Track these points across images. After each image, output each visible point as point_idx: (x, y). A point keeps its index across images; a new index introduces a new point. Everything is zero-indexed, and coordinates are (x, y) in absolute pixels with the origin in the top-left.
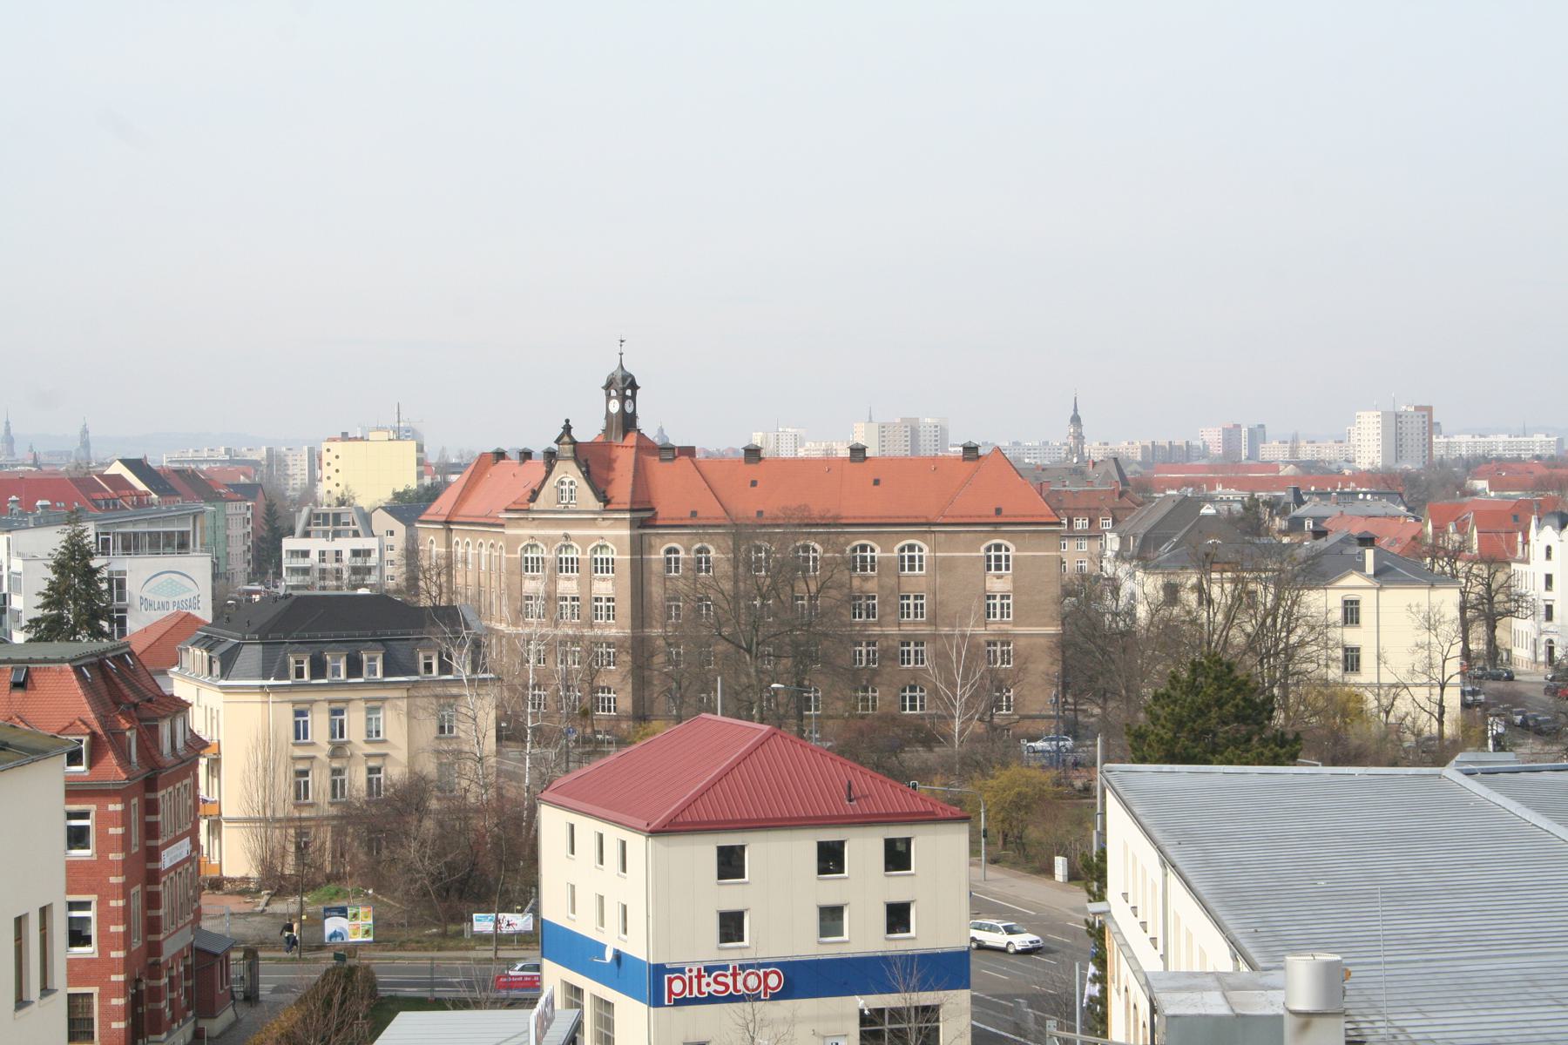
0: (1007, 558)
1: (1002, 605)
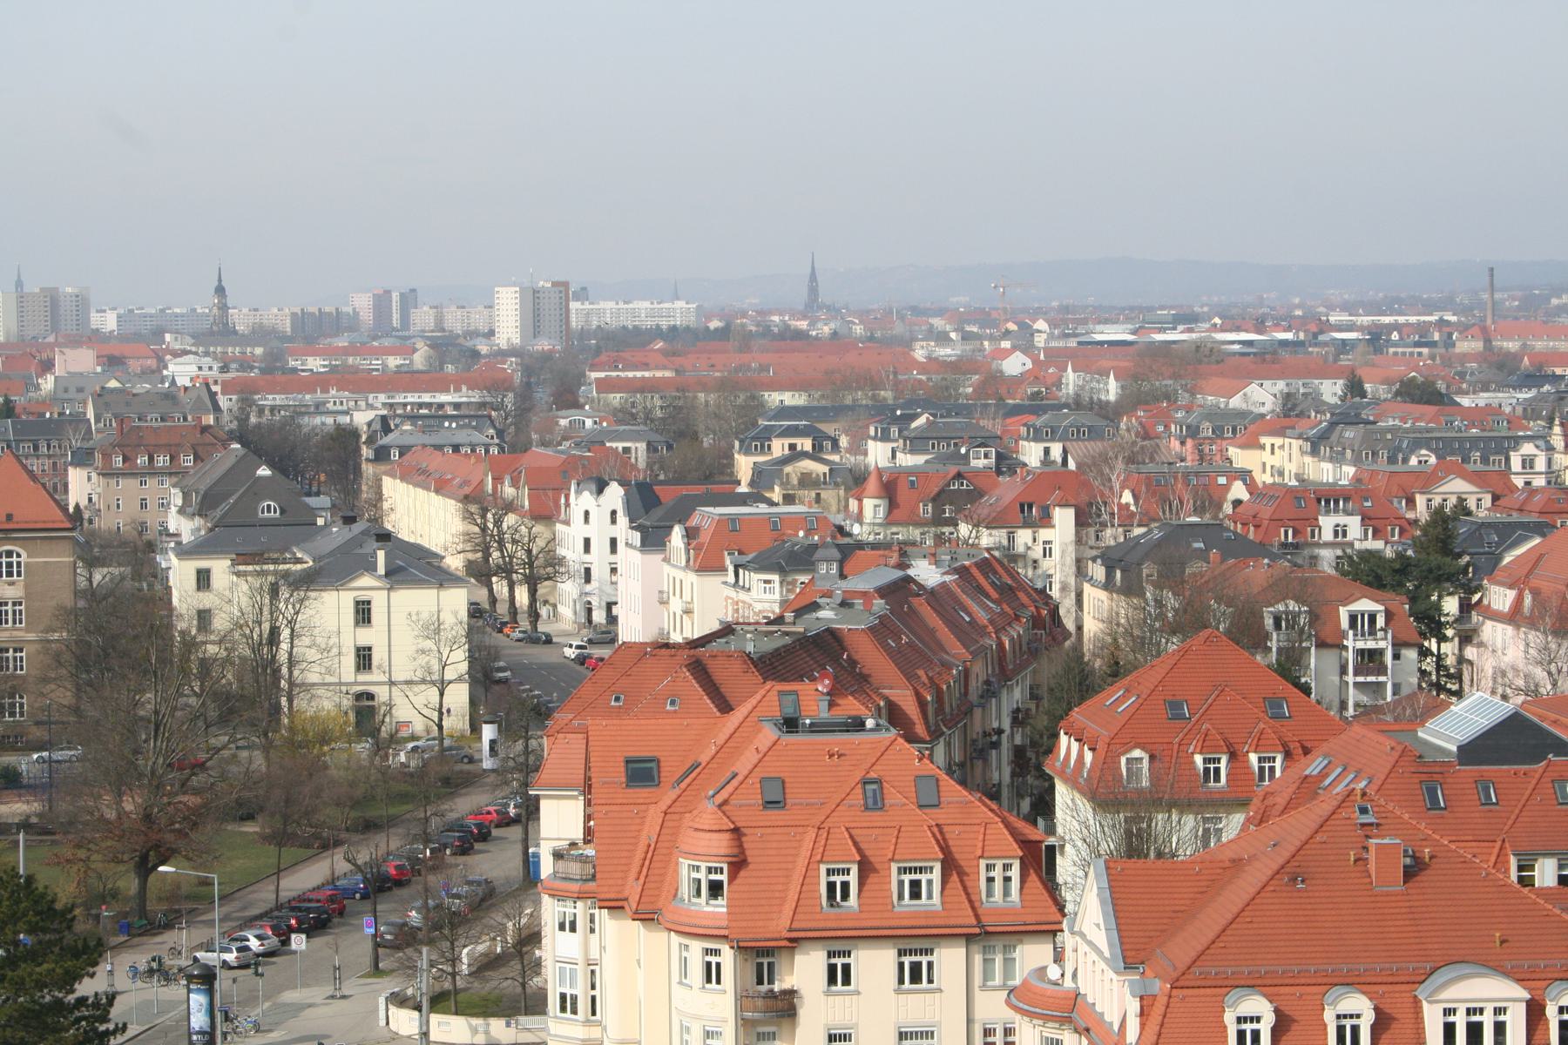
0: (19, 564)
1: (14, 612)
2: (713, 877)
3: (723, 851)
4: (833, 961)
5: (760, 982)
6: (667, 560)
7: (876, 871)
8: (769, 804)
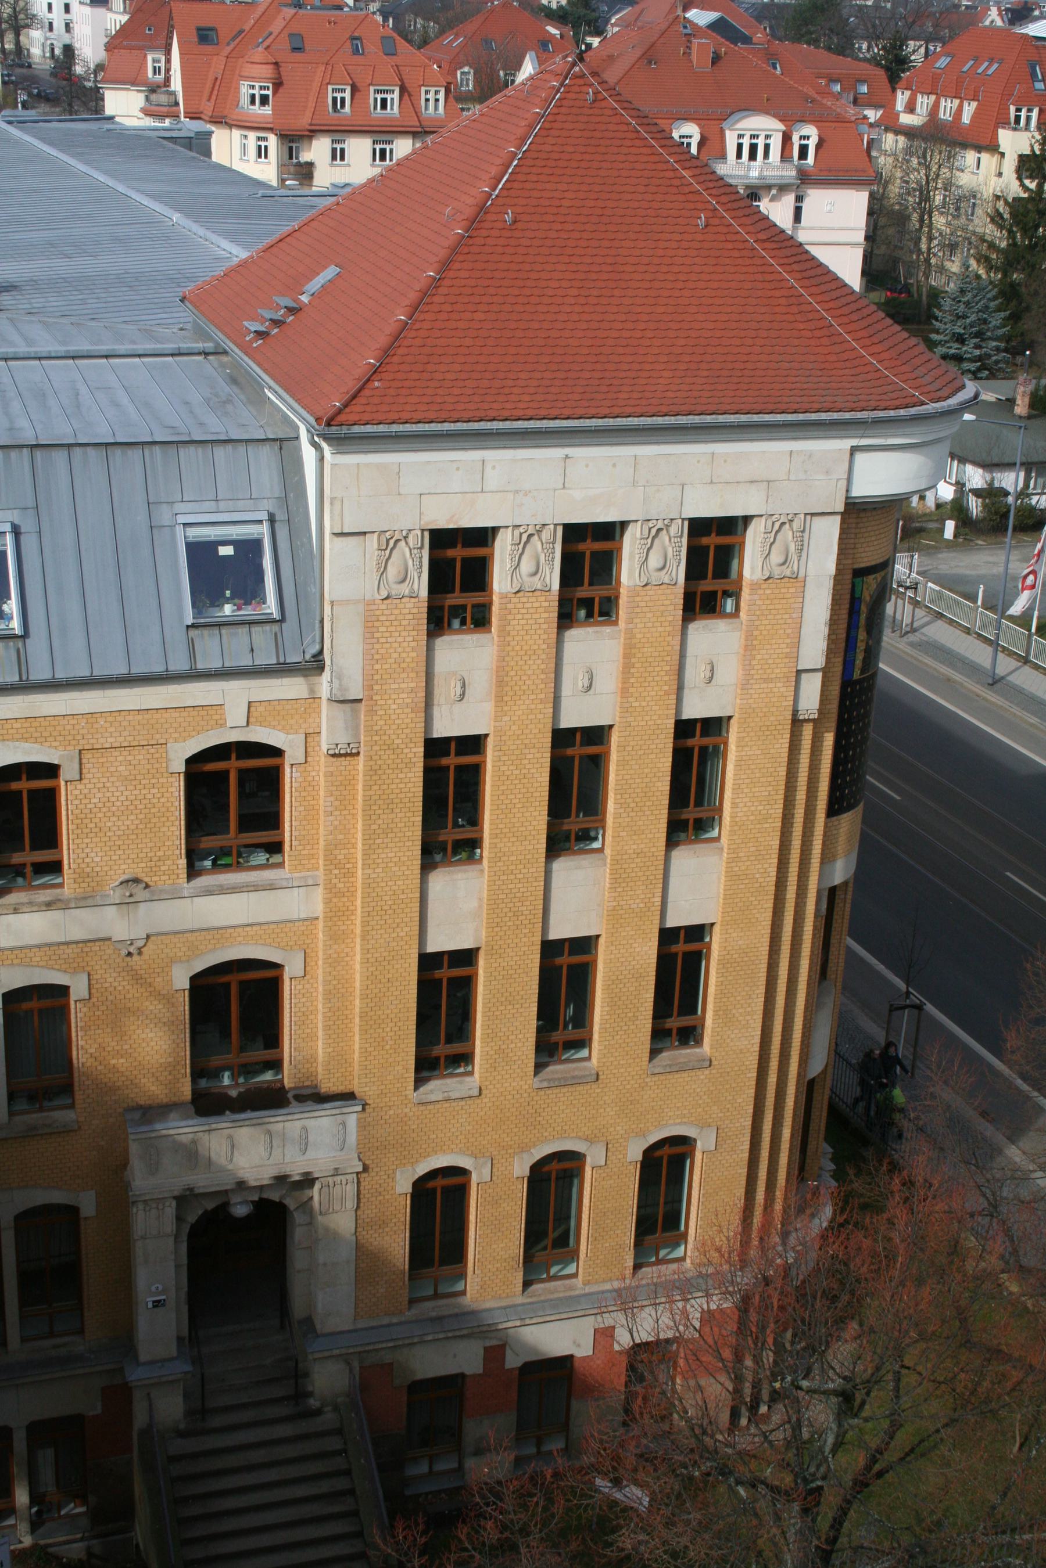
2: (263, 92)
3: (269, 76)
4: (335, 146)
5: (291, 158)
6: (110, 10)
7: (359, 91)
8: (296, 49)
